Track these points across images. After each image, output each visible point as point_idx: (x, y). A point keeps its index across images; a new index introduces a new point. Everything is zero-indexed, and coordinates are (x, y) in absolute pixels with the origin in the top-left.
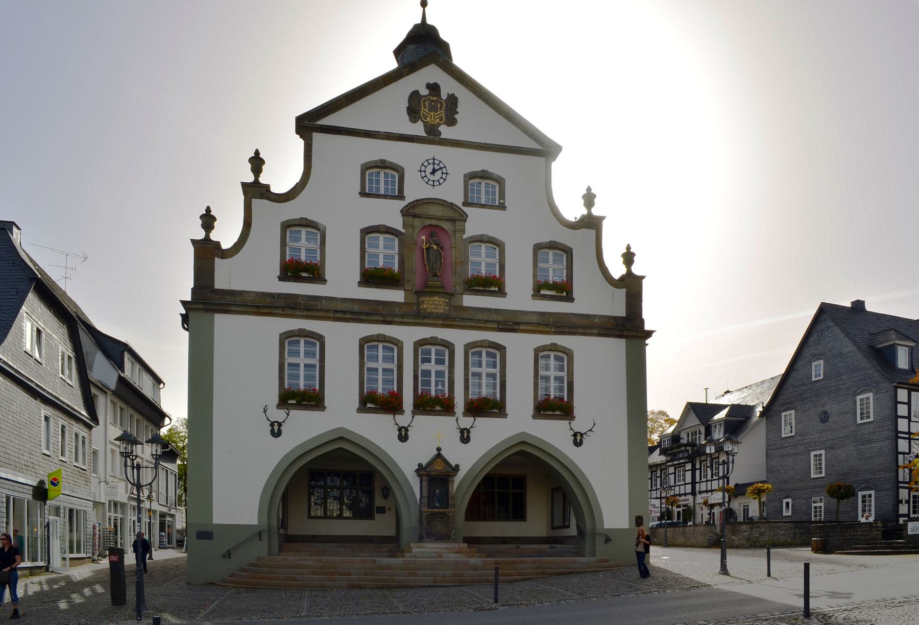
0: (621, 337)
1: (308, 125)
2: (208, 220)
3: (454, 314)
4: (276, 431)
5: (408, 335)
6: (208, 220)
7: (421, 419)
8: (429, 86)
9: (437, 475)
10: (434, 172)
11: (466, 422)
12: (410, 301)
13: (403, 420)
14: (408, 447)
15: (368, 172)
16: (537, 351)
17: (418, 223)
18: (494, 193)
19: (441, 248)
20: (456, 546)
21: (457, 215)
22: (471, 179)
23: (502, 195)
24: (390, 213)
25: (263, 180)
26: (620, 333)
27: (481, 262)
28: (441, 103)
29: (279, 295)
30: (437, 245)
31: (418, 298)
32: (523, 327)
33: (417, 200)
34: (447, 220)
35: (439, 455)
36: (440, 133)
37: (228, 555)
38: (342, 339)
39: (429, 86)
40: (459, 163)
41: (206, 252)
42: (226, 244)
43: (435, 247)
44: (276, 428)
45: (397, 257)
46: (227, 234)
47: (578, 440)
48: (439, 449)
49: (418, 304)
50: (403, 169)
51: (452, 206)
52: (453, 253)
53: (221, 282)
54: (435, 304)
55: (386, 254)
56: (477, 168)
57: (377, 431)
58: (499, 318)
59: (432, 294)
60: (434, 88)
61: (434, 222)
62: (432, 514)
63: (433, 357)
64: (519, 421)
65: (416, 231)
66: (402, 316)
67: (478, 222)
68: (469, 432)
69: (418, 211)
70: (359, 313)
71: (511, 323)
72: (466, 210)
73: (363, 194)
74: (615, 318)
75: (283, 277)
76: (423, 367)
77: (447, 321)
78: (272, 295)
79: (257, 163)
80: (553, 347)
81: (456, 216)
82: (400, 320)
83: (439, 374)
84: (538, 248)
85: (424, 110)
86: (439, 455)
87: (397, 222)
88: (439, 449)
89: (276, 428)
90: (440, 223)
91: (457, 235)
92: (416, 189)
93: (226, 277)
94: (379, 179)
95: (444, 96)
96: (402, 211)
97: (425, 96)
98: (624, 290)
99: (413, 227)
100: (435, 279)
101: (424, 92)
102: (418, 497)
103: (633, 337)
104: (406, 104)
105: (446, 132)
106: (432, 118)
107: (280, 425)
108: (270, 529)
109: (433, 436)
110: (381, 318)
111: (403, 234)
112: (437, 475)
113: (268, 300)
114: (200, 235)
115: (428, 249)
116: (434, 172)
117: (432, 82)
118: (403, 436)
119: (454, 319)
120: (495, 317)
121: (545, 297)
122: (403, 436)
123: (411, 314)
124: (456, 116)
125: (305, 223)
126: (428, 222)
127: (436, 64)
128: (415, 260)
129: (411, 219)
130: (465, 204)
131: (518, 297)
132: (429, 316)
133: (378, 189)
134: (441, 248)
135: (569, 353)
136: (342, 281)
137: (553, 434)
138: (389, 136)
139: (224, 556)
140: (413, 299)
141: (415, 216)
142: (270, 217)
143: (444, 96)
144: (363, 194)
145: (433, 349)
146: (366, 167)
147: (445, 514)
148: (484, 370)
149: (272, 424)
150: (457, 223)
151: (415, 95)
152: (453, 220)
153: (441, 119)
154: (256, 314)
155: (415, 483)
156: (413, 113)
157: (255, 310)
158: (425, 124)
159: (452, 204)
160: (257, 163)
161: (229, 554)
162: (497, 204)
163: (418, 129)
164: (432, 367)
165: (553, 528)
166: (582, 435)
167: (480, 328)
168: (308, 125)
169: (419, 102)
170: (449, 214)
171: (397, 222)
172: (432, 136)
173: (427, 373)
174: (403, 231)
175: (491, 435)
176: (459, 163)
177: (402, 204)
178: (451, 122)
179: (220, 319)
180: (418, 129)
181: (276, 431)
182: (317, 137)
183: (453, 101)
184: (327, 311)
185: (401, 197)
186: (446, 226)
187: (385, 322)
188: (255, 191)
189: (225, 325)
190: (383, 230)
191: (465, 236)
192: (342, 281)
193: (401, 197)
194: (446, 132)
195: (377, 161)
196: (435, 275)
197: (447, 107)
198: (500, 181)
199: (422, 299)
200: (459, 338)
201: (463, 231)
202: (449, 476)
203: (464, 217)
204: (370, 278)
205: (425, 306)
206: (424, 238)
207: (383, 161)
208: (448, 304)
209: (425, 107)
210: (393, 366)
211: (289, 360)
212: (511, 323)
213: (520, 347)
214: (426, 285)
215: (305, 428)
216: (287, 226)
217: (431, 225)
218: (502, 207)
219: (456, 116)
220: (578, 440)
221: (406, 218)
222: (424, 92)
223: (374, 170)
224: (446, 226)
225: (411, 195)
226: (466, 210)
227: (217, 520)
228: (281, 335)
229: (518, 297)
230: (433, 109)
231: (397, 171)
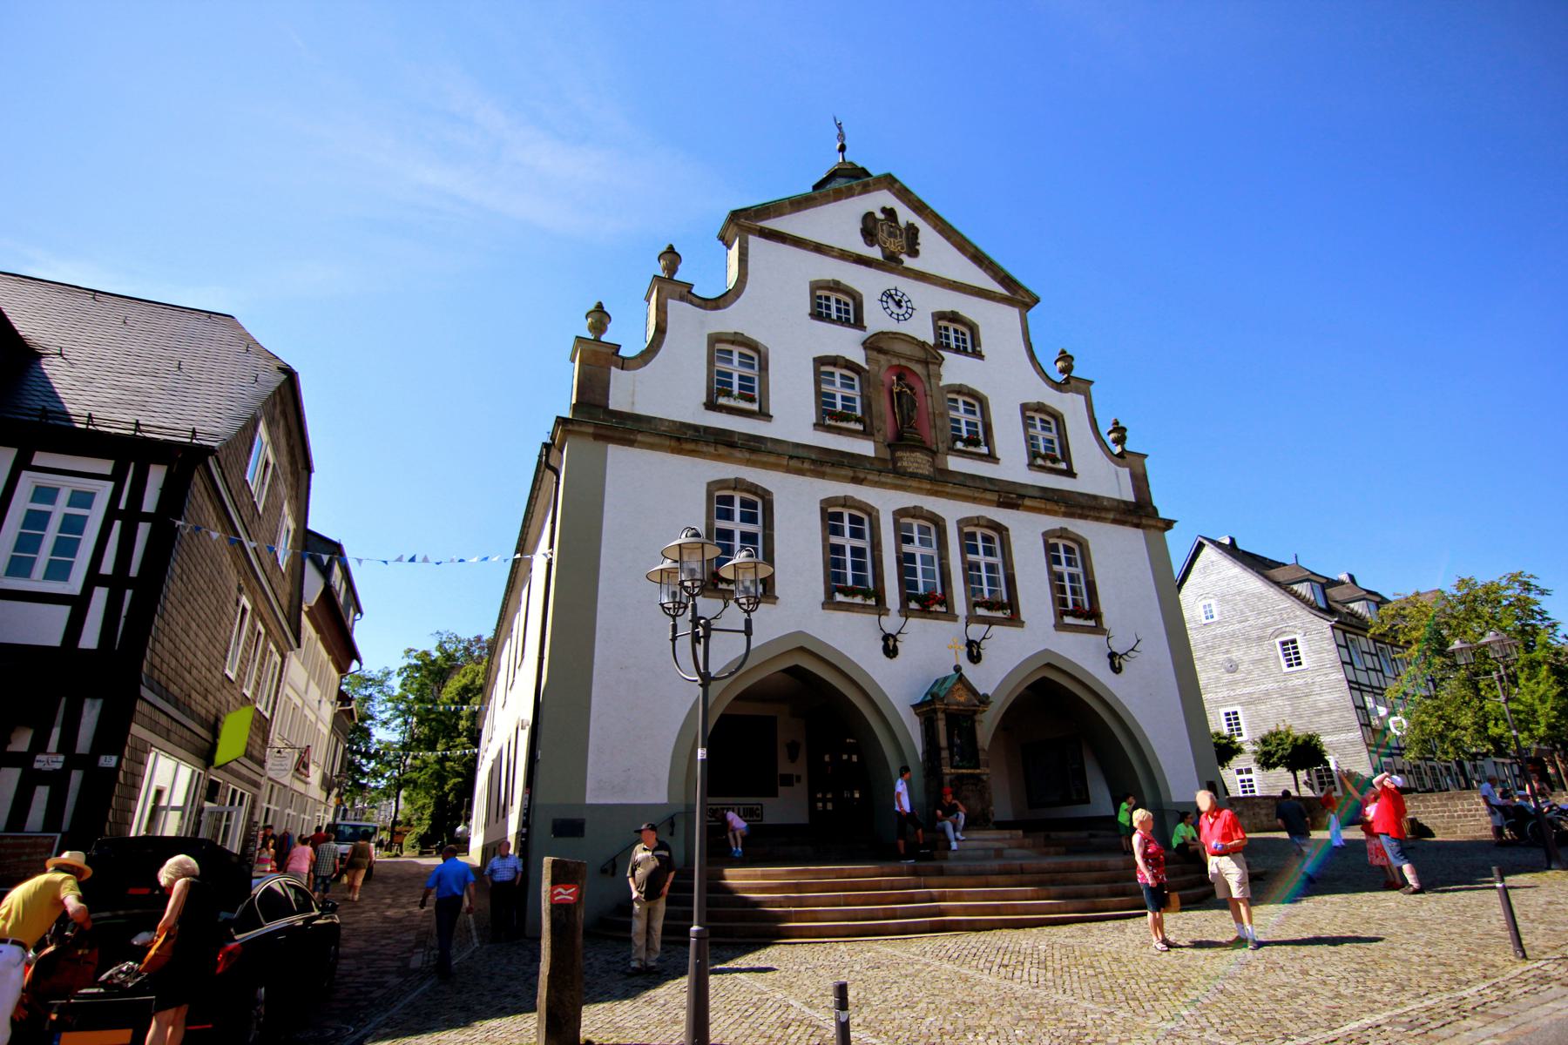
0: (1137, 526)
2: (600, 317)
5: (886, 501)
6: (600, 317)
7: (914, 622)
8: (884, 210)
11: (976, 631)
13: (892, 622)
14: (898, 664)
24: (847, 343)
26: (1136, 521)
32: (1028, 502)
33: (883, 333)
34: (919, 361)
39: (884, 210)
45: (858, 400)
46: (630, 335)
49: (894, 460)
51: (923, 344)
53: (618, 400)
54: (914, 461)
56: (947, 308)
57: (850, 637)
60: (890, 213)
61: (903, 362)
62: (960, 777)
67: (955, 370)
68: (978, 644)
69: (884, 345)
74: (1125, 502)
76: (907, 548)
78: (696, 428)
83: (927, 560)
90: (910, 365)
92: (877, 319)
93: (626, 393)
99: (878, 362)
104: (859, 226)
106: (893, 245)
109: (931, 648)
112: (947, 710)
113: (690, 433)
118: (890, 648)
121: (1042, 468)
122: (890, 648)
125: (739, 340)
126: (895, 362)
128: (883, 404)
135: (1082, 544)
137: (1081, 652)
138: (844, 255)
140: (887, 454)
141: (880, 351)
151: (868, 217)
152: (926, 363)
154: (674, 451)
157: (673, 443)
163: (875, 253)
167: (974, 500)
170: (920, 354)
171: (858, 356)
172: (890, 263)
178: (914, 253)
180: (875, 253)
183: (912, 232)
186: (917, 368)
189: (622, 462)
193: (863, 328)
194: (908, 262)
198: (973, 328)
199: (899, 454)
200: (952, 511)
201: (939, 377)
202: (975, 712)
207: (837, 283)
208: (933, 465)
212: (1011, 496)
216: (714, 339)
217: (899, 366)
220: (1115, 662)
222: (880, 216)
224: (917, 368)
229: (1012, 465)
230: (891, 235)
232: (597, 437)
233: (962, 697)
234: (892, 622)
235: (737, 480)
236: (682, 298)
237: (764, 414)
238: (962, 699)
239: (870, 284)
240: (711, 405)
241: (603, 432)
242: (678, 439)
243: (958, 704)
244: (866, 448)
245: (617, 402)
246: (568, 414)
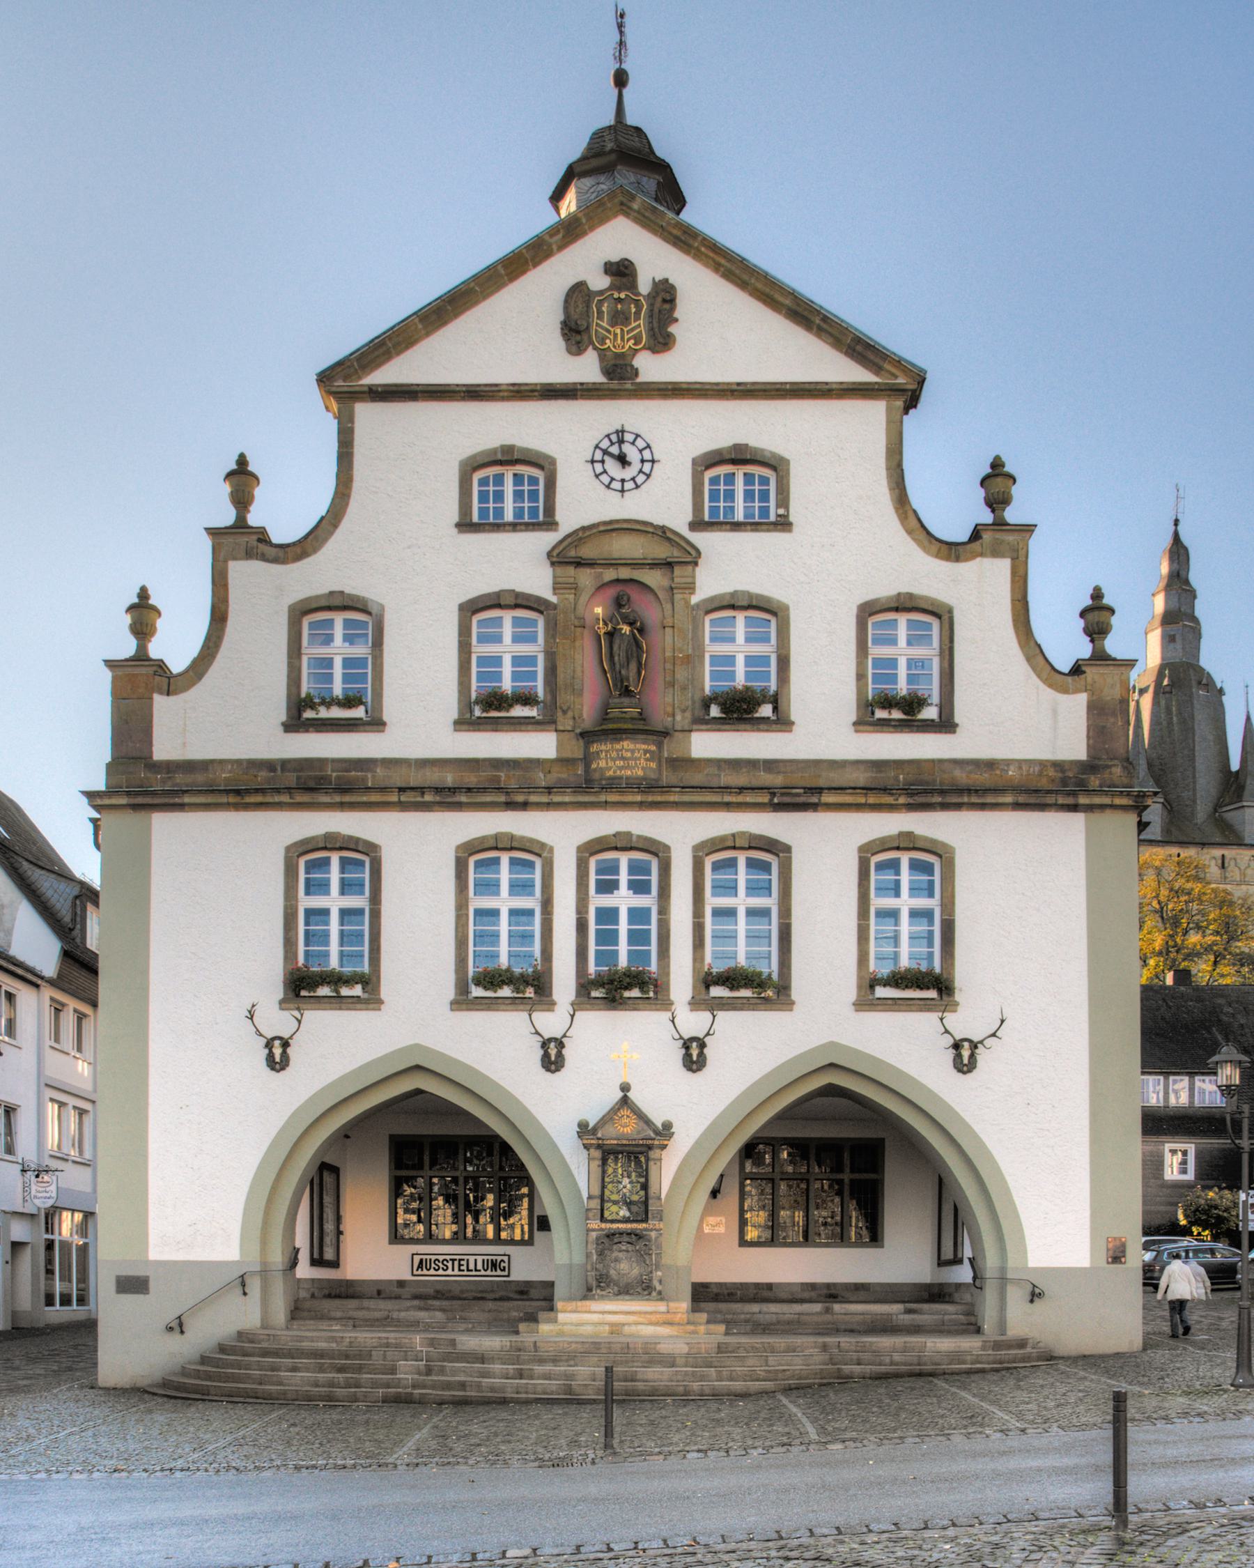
0: (1074, 808)
1: (348, 384)
2: (143, 615)
3: (667, 777)
4: (278, 1056)
5: (563, 831)
6: (143, 615)
9: (626, 1147)
10: (623, 460)
11: (693, 1023)
12: (569, 755)
13: (551, 1023)
15: (477, 476)
16: (866, 852)
17: (586, 578)
18: (764, 496)
19: (641, 631)
20: (662, 1307)
21: (676, 553)
22: (708, 467)
23: (784, 501)
24: (521, 563)
25: (253, 519)
26: (1070, 801)
27: (734, 653)
28: (637, 302)
29: (285, 764)
30: (631, 624)
31: (587, 747)
32: (828, 798)
33: (583, 529)
34: (654, 565)
35: (625, 1101)
36: (636, 373)
37: (178, 1326)
38: (419, 852)
40: (679, 436)
41: (139, 683)
42: (178, 663)
43: (626, 629)
44: (277, 1051)
47: (964, 1056)
48: (625, 1088)
49: (587, 759)
50: (553, 462)
51: (663, 534)
52: (669, 640)
54: (626, 758)
55: (512, 651)
56: (723, 440)
57: (492, 1053)
58: (777, 780)
59: (617, 734)
60: (621, 271)
61: (625, 573)
62: (610, 1235)
63: (624, 877)
64: (825, 1020)
65: (584, 598)
66: (549, 790)
67: (727, 564)
68: (702, 1045)
69: (587, 552)
70: (453, 790)
71: (802, 790)
72: (698, 538)
73: (466, 525)
74: (1058, 765)
75: (465, 723)
77: (649, 793)
78: (269, 765)
79: (242, 478)
80: (907, 842)
81: (676, 554)
82: (545, 799)
83: (637, 915)
84: (867, 611)
85: (600, 324)
86: (625, 1101)
87: (537, 580)
88: (625, 1088)
89: (277, 1051)
91: (677, 597)
92: (582, 501)
93: (179, 732)
94: (503, 488)
95: (644, 287)
96: (549, 555)
97: (601, 292)
98: (1082, 698)
99: (575, 588)
100: (626, 700)
101: (599, 282)
102: (585, 1195)
103: (1102, 807)
105: (650, 367)
107: (285, 1044)
108: (265, 1273)
109: (622, 1056)
110: (502, 799)
111: (555, 607)
113: (263, 774)
114: (126, 647)
115: (611, 635)
116: (623, 460)
117: (615, 258)
119: (669, 788)
120: (766, 779)
121: (884, 725)
123: (580, 786)
124: (672, 329)
126: (610, 575)
127: (627, 215)
129: (571, 570)
130: (698, 524)
131: (822, 724)
132: (612, 785)
133: (499, 512)
134: (641, 631)
135: (944, 854)
136: (421, 720)
137: (903, 1048)
138: (520, 393)
139: (171, 1329)
140: (575, 749)
141: (579, 563)
142: (264, 592)
143: (644, 287)
144: (466, 525)
145: (624, 859)
146: (471, 467)
147: (639, 1236)
148: (742, 901)
149: (269, 1045)
150: (678, 571)
151: (578, 293)
153: (637, 340)
154: (238, 807)
155: (579, 1167)
156: (575, 333)
157: (232, 799)
158: (602, 354)
159: (664, 529)
160: (242, 478)
161: (181, 1325)
162: (509, 516)
163: (587, 369)
164: (623, 900)
165: (941, 1263)
166: (974, 1046)
167: (728, 806)
168: (348, 384)
169: (588, 306)
170: (662, 551)
172: (619, 380)
173: (608, 915)
174: (554, 599)
175: (756, 1054)
176: (679, 436)
177: (548, 539)
178: (661, 341)
179: (163, 824)
180: (587, 369)
181: (278, 1056)
182: (365, 413)
183: (665, 294)
184: (383, 790)
185: (549, 524)
186: (654, 578)
187: (510, 806)
188: (239, 541)
190: (511, 601)
191: (694, 600)
192: (421, 720)
193: (549, 524)
194: (650, 367)
195: (495, 451)
196: (627, 692)
197: (651, 311)
198: (777, 465)
199: (594, 748)
200: (682, 831)
201: (691, 588)
202: (650, 1147)
203: (692, 557)
204: (487, 708)
205: (602, 764)
206: (599, 610)
207: (508, 449)
208: (656, 757)
209: (600, 317)
210: (532, 902)
211: (306, 902)
212: (802, 790)
213: (826, 849)
214: (605, 716)
215: (342, 1050)
216: (301, 611)
217: (618, 581)
218: (783, 524)
219: (672, 329)
220: (964, 1056)
221: (560, 570)
222: (599, 282)
223: (491, 471)
224: (654, 578)
225: (570, 517)
226: (698, 538)
227: (157, 1252)
228: (288, 849)
230: (620, 318)
231: (541, 467)
232: (136, 807)
233: (627, 1128)
234: (551, 1023)
235: (329, 837)
236: (249, 554)
237: (376, 723)
238: (628, 1130)
239: (566, 434)
240: (296, 722)
241: (140, 800)
242: (238, 792)
243: (623, 1136)
244: (540, 745)
245: (163, 749)
246: (101, 786)
